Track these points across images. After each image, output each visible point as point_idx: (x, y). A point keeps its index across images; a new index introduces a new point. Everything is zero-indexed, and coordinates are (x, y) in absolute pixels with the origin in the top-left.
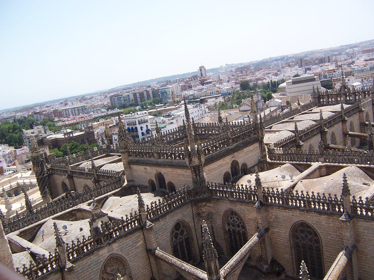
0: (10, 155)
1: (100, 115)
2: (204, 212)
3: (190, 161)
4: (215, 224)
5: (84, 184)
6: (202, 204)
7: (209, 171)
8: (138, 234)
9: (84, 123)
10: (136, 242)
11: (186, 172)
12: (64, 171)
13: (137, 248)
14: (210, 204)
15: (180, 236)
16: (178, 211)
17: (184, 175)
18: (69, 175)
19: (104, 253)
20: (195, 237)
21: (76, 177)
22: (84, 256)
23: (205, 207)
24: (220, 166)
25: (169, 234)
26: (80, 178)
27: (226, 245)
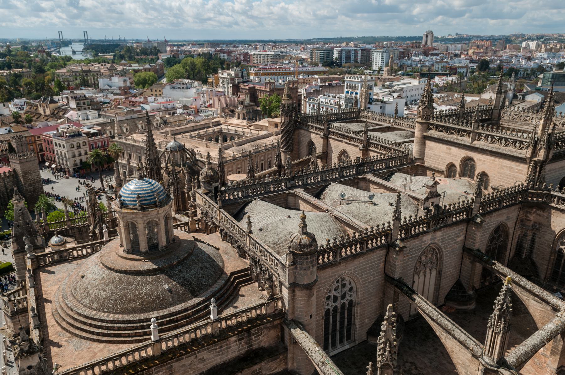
0: (205, 95)
1: (301, 69)
2: (530, 221)
3: (534, 154)
4: (539, 238)
5: (342, 149)
6: (532, 210)
7: (549, 171)
8: (463, 227)
9: (282, 75)
10: (457, 236)
11: (518, 166)
12: (316, 128)
13: (455, 243)
14: (543, 212)
15: (495, 242)
16: (504, 211)
17: (512, 168)
18: (324, 134)
19: (427, 239)
20: (509, 247)
21: (333, 139)
22: (411, 237)
23: (534, 215)
24: (561, 167)
25: (488, 235)
26: (338, 140)
27: (547, 268)
